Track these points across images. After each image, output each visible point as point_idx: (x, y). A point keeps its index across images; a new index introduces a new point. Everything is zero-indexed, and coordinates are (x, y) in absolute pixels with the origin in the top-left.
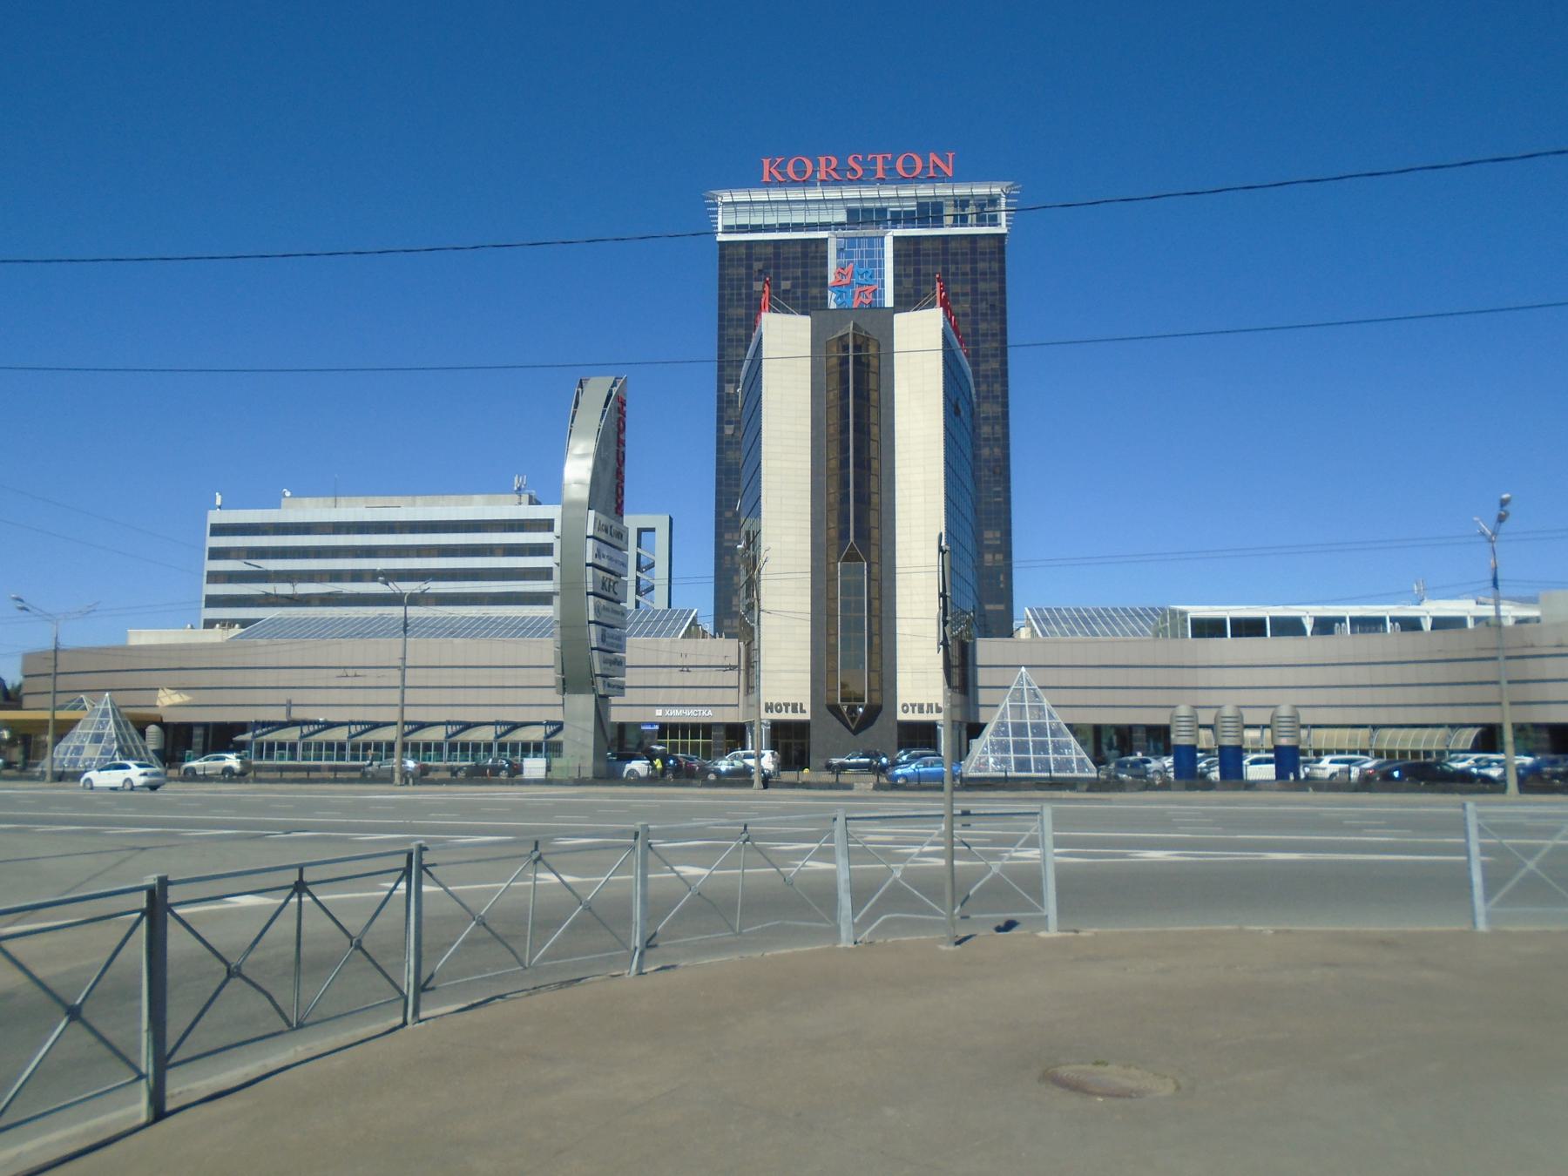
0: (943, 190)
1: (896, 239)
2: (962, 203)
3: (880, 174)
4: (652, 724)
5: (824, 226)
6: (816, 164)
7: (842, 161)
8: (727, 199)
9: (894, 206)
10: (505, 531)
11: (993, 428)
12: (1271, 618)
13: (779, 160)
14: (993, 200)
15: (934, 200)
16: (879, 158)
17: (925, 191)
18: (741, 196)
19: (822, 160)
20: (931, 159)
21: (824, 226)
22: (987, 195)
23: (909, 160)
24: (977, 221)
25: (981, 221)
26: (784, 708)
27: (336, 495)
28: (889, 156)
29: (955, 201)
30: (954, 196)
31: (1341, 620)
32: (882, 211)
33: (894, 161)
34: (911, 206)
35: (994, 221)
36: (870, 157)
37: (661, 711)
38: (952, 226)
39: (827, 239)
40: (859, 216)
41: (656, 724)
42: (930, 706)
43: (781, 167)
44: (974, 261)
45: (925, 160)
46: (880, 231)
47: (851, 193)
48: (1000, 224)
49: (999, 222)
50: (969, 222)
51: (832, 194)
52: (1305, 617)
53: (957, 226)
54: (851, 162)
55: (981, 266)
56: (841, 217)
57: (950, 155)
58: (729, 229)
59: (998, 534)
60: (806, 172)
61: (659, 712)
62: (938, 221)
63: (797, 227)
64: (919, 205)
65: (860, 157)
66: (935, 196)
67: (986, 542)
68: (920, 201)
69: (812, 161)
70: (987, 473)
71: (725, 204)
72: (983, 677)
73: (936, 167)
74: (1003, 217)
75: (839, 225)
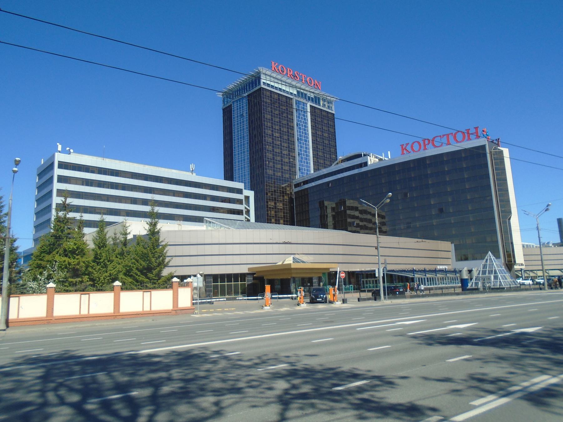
5: (291, 93)
9: (309, 94)
13: (277, 64)
16: (303, 75)
19: (288, 69)
27: (104, 157)
29: (323, 99)
34: (312, 96)
42: (521, 264)
43: (277, 66)
56: (295, 92)
73: (317, 85)
74: (333, 108)
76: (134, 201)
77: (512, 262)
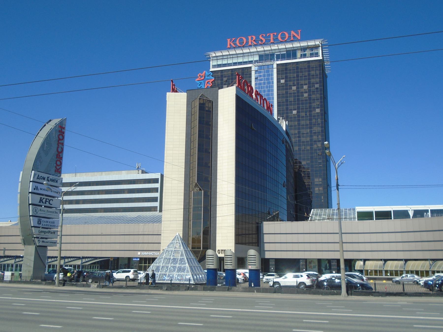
0: (296, 45)
1: (278, 65)
2: (304, 49)
3: (272, 41)
4: (137, 258)
5: (251, 62)
6: (247, 39)
7: (257, 37)
8: (214, 55)
10: (128, 184)
11: (318, 137)
12: (375, 212)
13: (233, 39)
14: (316, 47)
15: (293, 49)
16: (272, 35)
17: (289, 46)
18: (219, 54)
19: (250, 37)
20: (292, 33)
21: (251, 62)
23: (283, 35)
24: (310, 55)
25: (312, 55)
26: (221, 251)
28: (275, 34)
30: (300, 46)
31: (427, 211)
33: (277, 35)
35: (317, 55)
36: (268, 34)
37: (140, 253)
38: (300, 58)
39: (251, 67)
40: (263, 57)
41: (138, 258)
44: (309, 71)
45: (289, 34)
46: (272, 63)
47: (260, 49)
48: (319, 56)
49: (319, 55)
50: (307, 56)
51: (253, 50)
52: (409, 210)
53: (302, 58)
54: (261, 37)
55: (313, 73)
56: (257, 58)
57: (299, 31)
58: (214, 66)
59: (320, 180)
60: (243, 43)
61: (139, 253)
62: (295, 57)
63: (240, 63)
64: (287, 51)
65: (264, 35)
66: (293, 47)
67: (316, 183)
68: (287, 49)
69: (246, 38)
70: (315, 155)
71: (213, 57)
72: (266, 238)
75: (256, 61)
76: (77, 202)
77: (200, 248)
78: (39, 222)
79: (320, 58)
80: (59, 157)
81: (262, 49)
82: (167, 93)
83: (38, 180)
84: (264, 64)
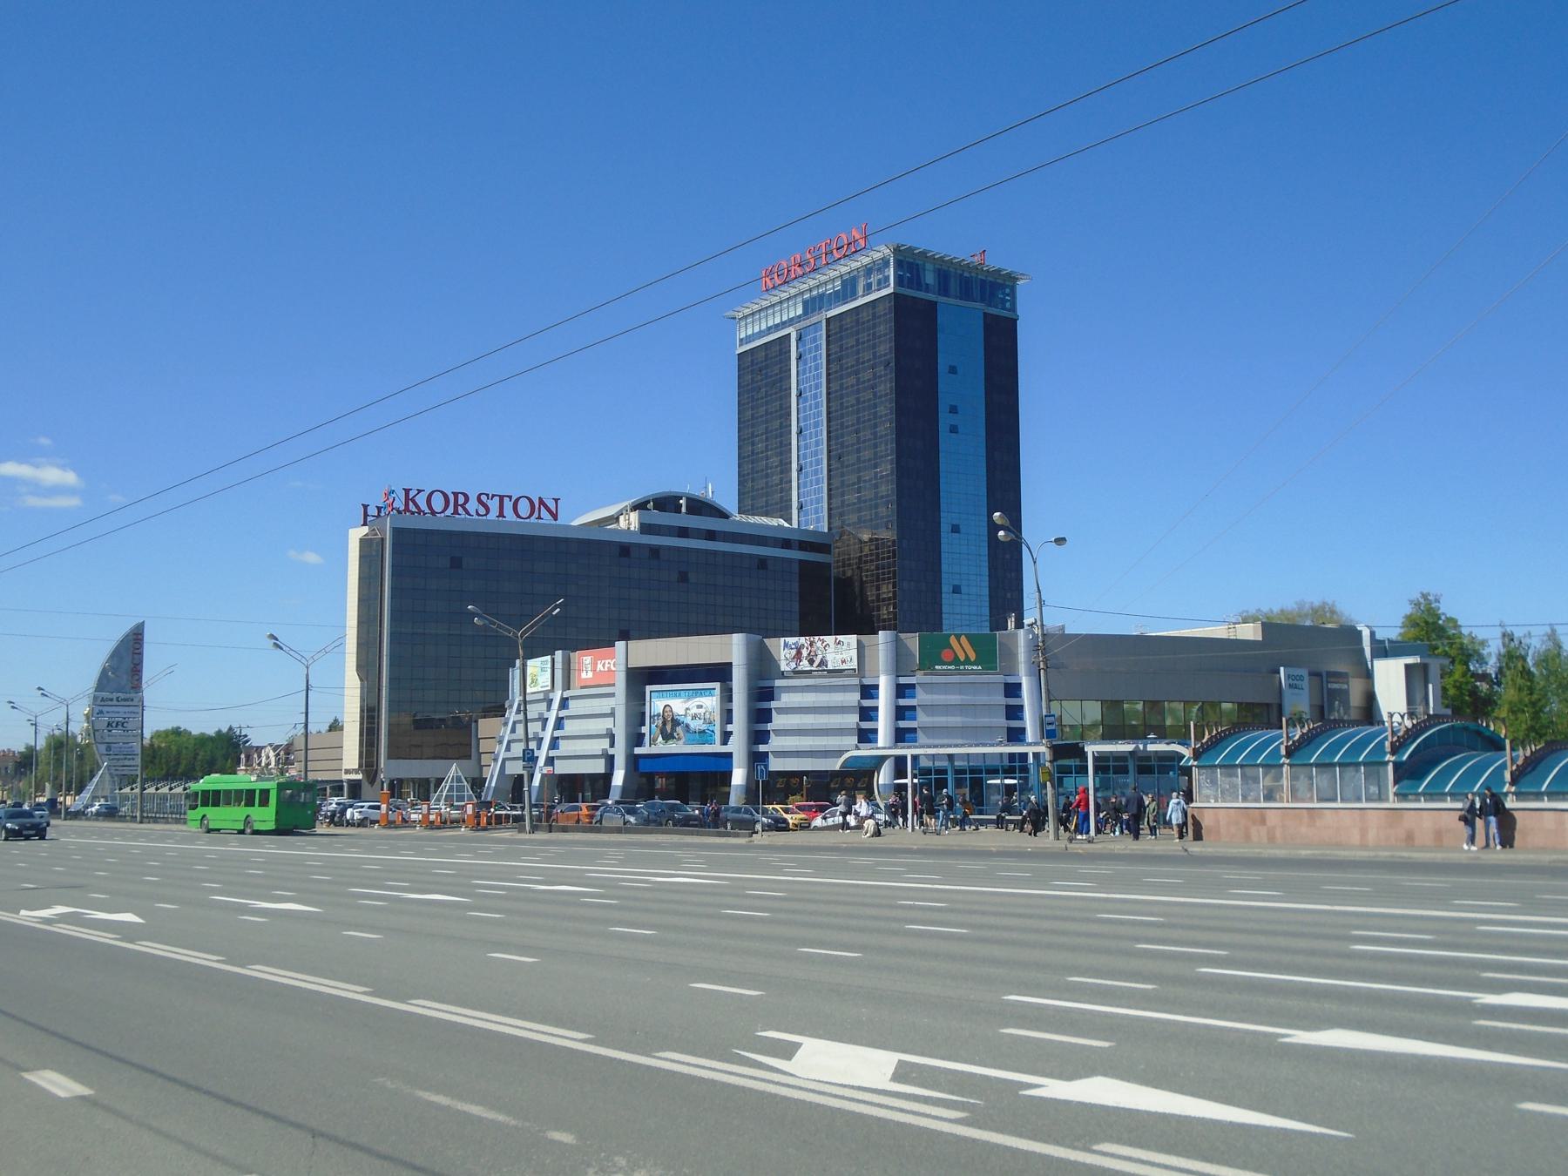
1: (828, 320)
2: (868, 271)
5: (790, 322)
9: (829, 289)
14: (886, 263)
22: (882, 259)
32: (821, 296)
35: (883, 283)
38: (863, 296)
39: (790, 334)
40: (812, 306)
59: (890, 586)
64: (844, 283)
67: (885, 596)
78: (109, 749)
79: (890, 290)
80: (136, 670)
81: (805, 287)
82: (350, 530)
83: (103, 703)
84: (808, 322)
